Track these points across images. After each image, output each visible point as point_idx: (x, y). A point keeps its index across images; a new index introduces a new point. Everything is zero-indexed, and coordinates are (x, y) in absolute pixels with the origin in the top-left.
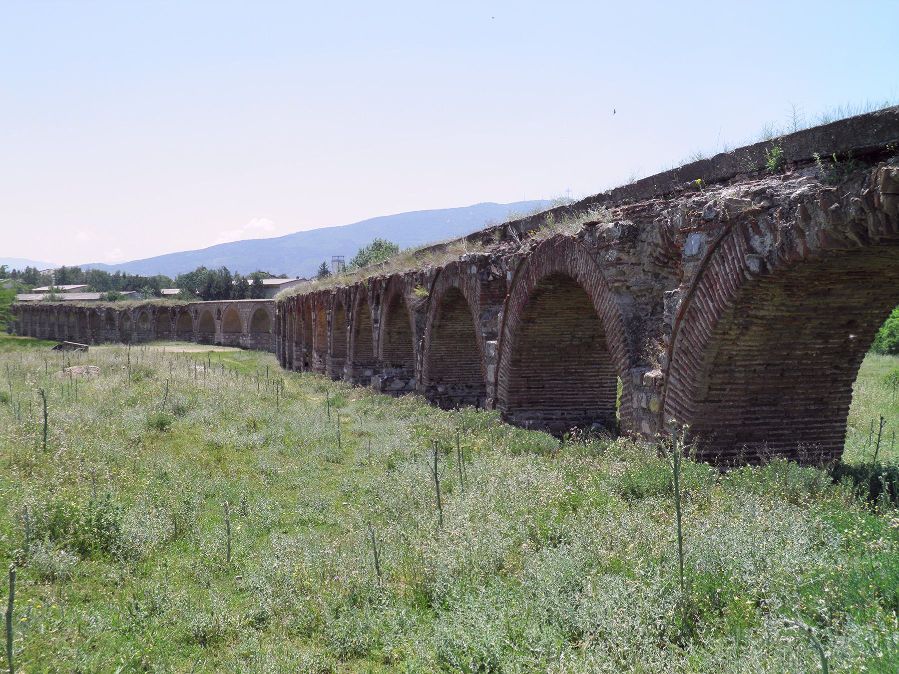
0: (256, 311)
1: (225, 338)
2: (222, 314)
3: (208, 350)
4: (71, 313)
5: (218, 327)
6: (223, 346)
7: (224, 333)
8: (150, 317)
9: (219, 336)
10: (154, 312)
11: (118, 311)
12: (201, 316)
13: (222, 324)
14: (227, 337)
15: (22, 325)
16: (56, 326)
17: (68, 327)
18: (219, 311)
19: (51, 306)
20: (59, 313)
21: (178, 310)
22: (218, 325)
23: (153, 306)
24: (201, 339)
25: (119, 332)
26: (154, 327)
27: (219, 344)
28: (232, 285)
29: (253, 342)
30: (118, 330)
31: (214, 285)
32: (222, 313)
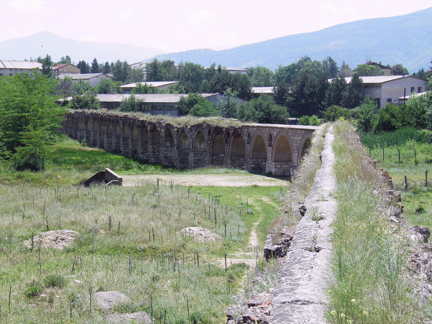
1: (276, 167)
3: (250, 185)
4: (135, 126)
7: (275, 162)
8: (206, 137)
9: (271, 166)
10: (209, 132)
11: (177, 127)
15: (92, 134)
16: (122, 139)
17: (132, 141)
18: (271, 136)
19: (117, 116)
20: (124, 124)
21: (232, 132)
22: (269, 152)
23: (209, 126)
25: (177, 151)
26: (209, 149)
27: (270, 175)
28: (328, 84)
30: (176, 148)
31: (308, 84)
32: (273, 139)
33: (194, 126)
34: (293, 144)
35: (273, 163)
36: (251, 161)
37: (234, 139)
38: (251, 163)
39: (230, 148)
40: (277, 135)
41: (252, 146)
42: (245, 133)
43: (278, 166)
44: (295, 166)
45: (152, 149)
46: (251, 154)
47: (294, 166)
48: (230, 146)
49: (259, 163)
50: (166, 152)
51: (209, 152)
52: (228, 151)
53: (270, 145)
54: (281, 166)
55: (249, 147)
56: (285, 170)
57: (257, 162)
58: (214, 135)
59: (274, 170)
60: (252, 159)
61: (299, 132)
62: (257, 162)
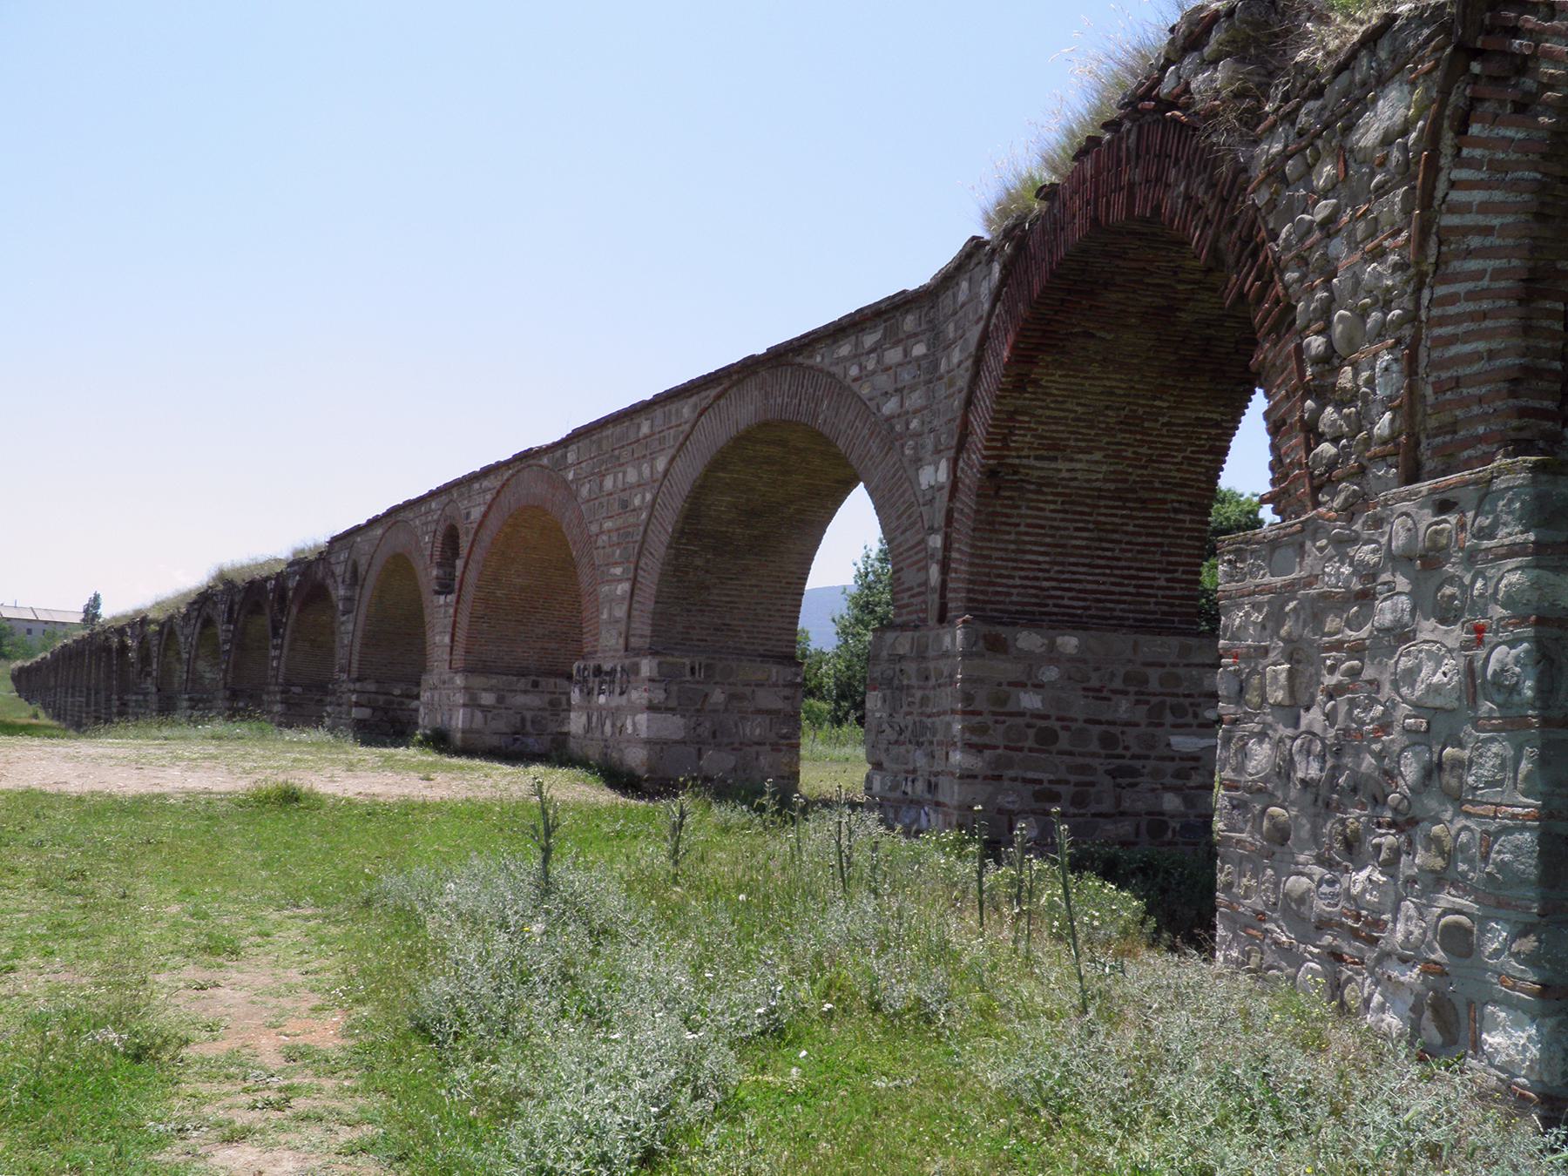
0: (718, 463)
1: (472, 704)
2: (464, 551)
3: (240, 784)
5: (439, 639)
6: (459, 752)
7: (469, 671)
10: (231, 610)
12: (371, 581)
13: (464, 621)
14: (488, 699)
18: (451, 538)
21: (292, 584)
24: (364, 713)
27: (440, 741)
29: (673, 726)
33: (195, 602)
34: (594, 528)
35: (459, 680)
36: (354, 691)
37: (300, 611)
38: (354, 698)
39: (285, 650)
40: (485, 515)
41: (361, 618)
42: (339, 570)
43: (488, 699)
44: (607, 667)
45: (117, 703)
46: (355, 658)
47: (598, 671)
48: (286, 642)
49: (391, 703)
50: (141, 707)
51: (225, 684)
52: (278, 668)
53: (445, 587)
54: (500, 700)
55: (350, 627)
56: (523, 720)
57: (381, 699)
58: (241, 618)
59: (459, 720)
60: (358, 680)
61: (645, 429)
62: (381, 699)
